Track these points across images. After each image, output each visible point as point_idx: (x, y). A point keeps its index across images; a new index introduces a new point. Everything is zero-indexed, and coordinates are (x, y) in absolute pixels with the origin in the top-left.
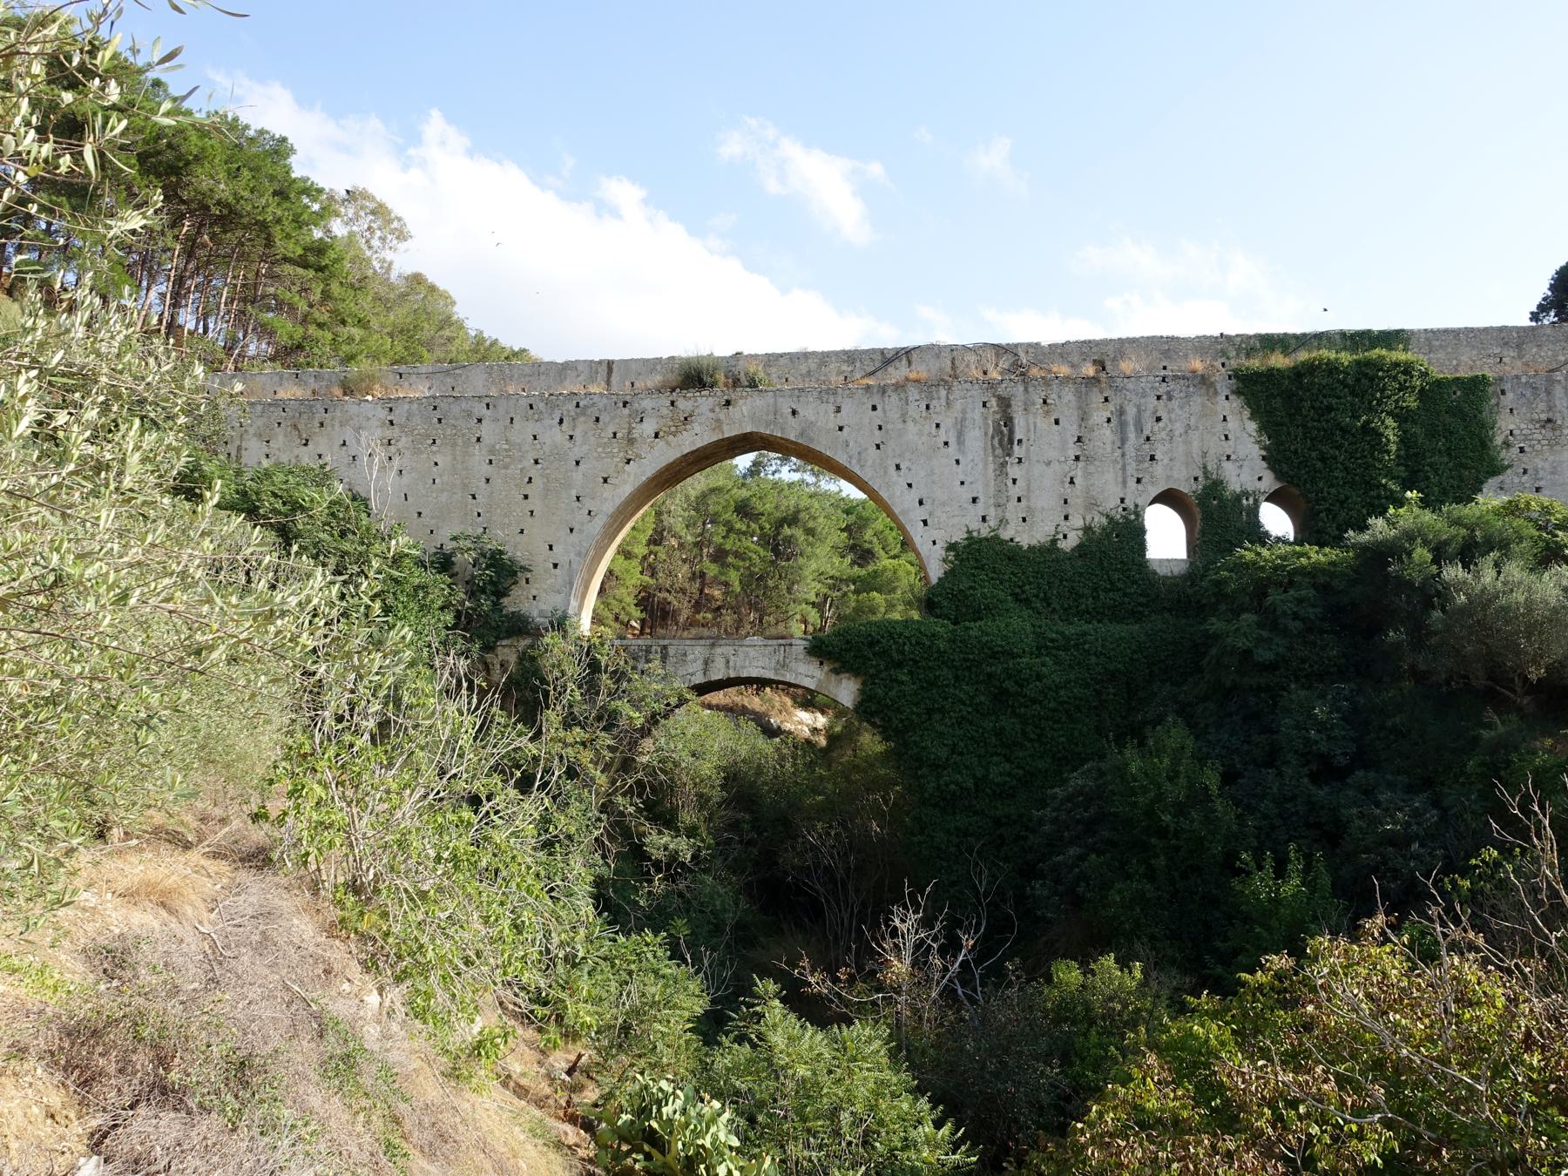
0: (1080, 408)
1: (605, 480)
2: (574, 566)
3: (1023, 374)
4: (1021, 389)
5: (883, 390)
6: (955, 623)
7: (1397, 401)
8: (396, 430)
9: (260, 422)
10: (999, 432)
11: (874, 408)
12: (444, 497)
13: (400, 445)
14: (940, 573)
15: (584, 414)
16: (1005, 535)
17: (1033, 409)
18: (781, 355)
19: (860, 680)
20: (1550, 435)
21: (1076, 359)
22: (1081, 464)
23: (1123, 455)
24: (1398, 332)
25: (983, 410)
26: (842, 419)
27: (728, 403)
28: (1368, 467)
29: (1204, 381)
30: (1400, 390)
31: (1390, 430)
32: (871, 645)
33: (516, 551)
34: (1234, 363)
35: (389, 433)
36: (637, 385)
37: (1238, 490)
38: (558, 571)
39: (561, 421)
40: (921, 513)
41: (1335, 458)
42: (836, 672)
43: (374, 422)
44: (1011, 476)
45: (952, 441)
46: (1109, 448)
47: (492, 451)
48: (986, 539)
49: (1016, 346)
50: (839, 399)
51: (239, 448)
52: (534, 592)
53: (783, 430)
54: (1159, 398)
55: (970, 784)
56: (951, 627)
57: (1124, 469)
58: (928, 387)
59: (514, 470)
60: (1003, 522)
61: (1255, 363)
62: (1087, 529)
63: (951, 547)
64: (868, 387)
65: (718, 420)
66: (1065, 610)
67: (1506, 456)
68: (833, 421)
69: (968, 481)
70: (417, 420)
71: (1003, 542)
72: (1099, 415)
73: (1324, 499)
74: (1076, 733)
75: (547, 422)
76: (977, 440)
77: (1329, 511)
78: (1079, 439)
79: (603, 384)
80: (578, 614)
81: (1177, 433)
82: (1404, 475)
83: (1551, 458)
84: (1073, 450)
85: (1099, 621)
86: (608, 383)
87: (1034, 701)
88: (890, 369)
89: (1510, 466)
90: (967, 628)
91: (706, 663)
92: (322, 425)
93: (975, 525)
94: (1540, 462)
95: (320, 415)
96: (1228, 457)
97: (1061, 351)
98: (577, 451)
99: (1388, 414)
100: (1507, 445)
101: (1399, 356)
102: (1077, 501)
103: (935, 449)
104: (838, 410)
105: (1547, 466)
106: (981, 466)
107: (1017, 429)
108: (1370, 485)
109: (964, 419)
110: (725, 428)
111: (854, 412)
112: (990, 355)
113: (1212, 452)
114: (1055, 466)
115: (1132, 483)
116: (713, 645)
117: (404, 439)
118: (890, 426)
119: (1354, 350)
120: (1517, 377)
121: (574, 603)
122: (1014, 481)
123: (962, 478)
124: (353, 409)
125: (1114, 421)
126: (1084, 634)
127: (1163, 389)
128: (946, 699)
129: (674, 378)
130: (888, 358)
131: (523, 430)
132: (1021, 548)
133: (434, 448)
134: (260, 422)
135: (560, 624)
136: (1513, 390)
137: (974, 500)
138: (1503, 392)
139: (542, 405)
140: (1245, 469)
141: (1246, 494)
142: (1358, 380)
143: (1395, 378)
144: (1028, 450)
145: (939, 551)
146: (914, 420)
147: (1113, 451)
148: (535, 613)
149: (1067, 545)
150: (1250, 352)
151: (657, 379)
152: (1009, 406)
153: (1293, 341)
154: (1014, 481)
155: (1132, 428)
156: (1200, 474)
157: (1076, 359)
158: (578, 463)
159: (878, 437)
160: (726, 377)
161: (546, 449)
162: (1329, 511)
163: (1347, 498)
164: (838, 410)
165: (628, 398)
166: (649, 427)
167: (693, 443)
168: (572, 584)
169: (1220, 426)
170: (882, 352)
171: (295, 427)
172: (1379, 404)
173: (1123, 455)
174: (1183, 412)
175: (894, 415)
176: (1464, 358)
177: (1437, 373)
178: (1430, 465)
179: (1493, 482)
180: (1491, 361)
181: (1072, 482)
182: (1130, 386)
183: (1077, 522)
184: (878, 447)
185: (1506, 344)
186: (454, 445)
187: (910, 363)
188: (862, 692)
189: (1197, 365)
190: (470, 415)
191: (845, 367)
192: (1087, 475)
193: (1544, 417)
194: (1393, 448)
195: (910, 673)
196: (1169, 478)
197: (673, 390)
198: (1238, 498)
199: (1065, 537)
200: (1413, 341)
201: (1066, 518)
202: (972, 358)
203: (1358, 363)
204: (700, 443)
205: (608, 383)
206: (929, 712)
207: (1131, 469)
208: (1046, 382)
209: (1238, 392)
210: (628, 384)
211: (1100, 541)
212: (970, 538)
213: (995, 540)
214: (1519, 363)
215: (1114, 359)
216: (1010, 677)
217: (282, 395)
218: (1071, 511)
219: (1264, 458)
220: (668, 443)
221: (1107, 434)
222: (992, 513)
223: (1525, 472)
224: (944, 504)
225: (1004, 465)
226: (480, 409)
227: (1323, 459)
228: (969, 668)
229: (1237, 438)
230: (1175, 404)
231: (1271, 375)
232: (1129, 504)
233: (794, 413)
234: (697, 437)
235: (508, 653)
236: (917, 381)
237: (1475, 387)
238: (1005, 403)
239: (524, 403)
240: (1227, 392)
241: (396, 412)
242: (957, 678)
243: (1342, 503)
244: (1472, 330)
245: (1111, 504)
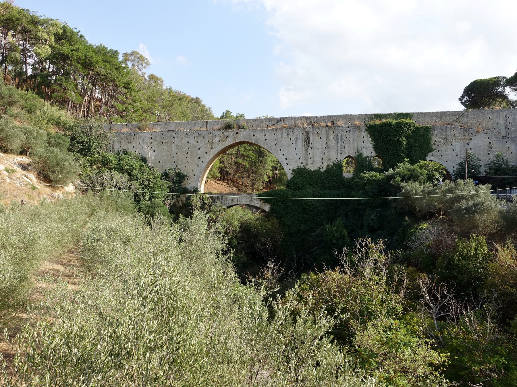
0: (327, 134)
1: (206, 153)
2: (199, 175)
3: (313, 125)
4: (312, 129)
5: (277, 130)
6: (294, 191)
7: (406, 133)
8: (153, 140)
9: (118, 138)
10: (306, 141)
11: (274, 134)
12: (165, 158)
13: (154, 144)
14: (291, 177)
16: (307, 167)
17: (315, 135)
18: (251, 120)
19: (270, 205)
20: (445, 141)
21: (327, 121)
22: (326, 149)
23: (337, 147)
24: (410, 113)
25: (302, 135)
26: (266, 137)
27: (237, 133)
28: (398, 150)
29: (358, 128)
30: (407, 130)
31: (404, 140)
33: (184, 172)
34: (367, 122)
35: (151, 141)
36: (214, 128)
37: (366, 156)
38: (195, 177)
39: (195, 138)
40: (286, 162)
41: (390, 148)
42: (264, 202)
43: (147, 138)
44: (309, 152)
46: (334, 145)
47: (177, 145)
48: (302, 169)
49: (311, 117)
50: (265, 132)
51: (113, 145)
52: (189, 182)
53: (251, 140)
54: (347, 132)
55: (296, 231)
56: (293, 191)
57: (337, 150)
58: (289, 128)
59: (183, 151)
60: (307, 164)
61: (372, 123)
62: (328, 166)
63: (294, 171)
64: (273, 129)
65: (235, 138)
66: (321, 187)
67: (434, 147)
68: (264, 138)
69: (298, 154)
70: (158, 137)
72: (331, 136)
73: (387, 159)
74: (322, 218)
75: (191, 138)
76: (300, 143)
77: (388, 162)
78: (326, 143)
79: (205, 127)
80: (200, 188)
82: (407, 152)
83: (445, 148)
84: (324, 146)
85: (330, 190)
86: (207, 127)
87: (312, 210)
88: (279, 123)
89: (435, 150)
90: (296, 192)
91: (232, 200)
92: (134, 139)
93: (300, 165)
94: (442, 149)
95: (133, 136)
96: (364, 147)
97: (323, 118)
98: (199, 146)
99: (404, 137)
100: (434, 144)
101: (408, 121)
102: (325, 159)
103: (290, 145)
104: (265, 135)
105: (444, 150)
106: (301, 149)
108: (398, 155)
109: (297, 137)
110: (236, 139)
111: (269, 136)
112: (304, 120)
113: (360, 146)
114: (320, 150)
115: (339, 154)
117: (155, 142)
118: (278, 139)
119: (396, 119)
120: (438, 126)
121: (199, 184)
122: (310, 153)
123: (297, 153)
124: (142, 135)
126: (325, 193)
127: (348, 129)
128: (291, 210)
129: (223, 126)
130: (279, 120)
131: (185, 140)
133: (163, 145)
134: (118, 138)
135: (196, 191)
136: (437, 130)
137: (300, 158)
138: (434, 130)
139: (190, 134)
140: (368, 151)
141: (368, 157)
142: (397, 128)
143: (406, 127)
144: (313, 146)
145: (291, 172)
146: (284, 138)
147: (335, 146)
148: (189, 187)
149: (323, 170)
150: (371, 119)
151: (218, 126)
152: (309, 134)
153: (383, 116)
154: (310, 153)
155: (340, 140)
156: (357, 152)
157: (327, 121)
158: (199, 149)
159: (275, 142)
160: (237, 126)
161: (191, 145)
162: (388, 162)
163: (392, 158)
165: (212, 132)
166: (217, 139)
167: (228, 143)
168: (199, 180)
169: (362, 139)
170: (277, 119)
171: (127, 139)
172: (402, 134)
173: (337, 147)
174: (351, 136)
175: (279, 136)
176: (426, 120)
177: (417, 126)
178: (414, 150)
179: (430, 154)
180: (433, 121)
181: (324, 154)
182: (339, 129)
183: (325, 164)
184: (275, 145)
185: (437, 116)
186: (168, 144)
187: (284, 121)
188: (270, 208)
189: (357, 123)
190: (171, 136)
191: (267, 123)
192: (328, 152)
193: (444, 137)
194: (404, 146)
195: (282, 203)
196: (349, 153)
197: (223, 130)
198: (366, 158)
200: (413, 115)
201: (323, 163)
202: (300, 121)
203: (397, 123)
204: (230, 144)
205: (207, 127)
206: (287, 213)
207: (339, 151)
208: (318, 128)
209: (367, 130)
210: (212, 127)
211: (331, 169)
212: (298, 168)
213: (305, 169)
214: (440, 122)
215: (336, 121)
216: (306, 204)
217: (123, 130)
218: (324, 161)
219: (373, 148)
220: (222, 144)
221: (333, 141)
222: (304, 162)
223: (439, 151)
224: (292, 160)
225: (307, 149)
227: (387, 148)
228: (297, 202)
229: (366, 142)
230: (351, 133)
231: (375, 126)
232: (339, 159)
233: (254, 136)
234: (230, 142)
235: (183, 197)
236: (285, 127)
237: (427, 129)
238: (308, 133)
239: (185, 133)
240: (364, 130)
241: (153, 135)
242: (294, 204)
243: (391, 160)
244: (429, 113)
245: (334, 159)
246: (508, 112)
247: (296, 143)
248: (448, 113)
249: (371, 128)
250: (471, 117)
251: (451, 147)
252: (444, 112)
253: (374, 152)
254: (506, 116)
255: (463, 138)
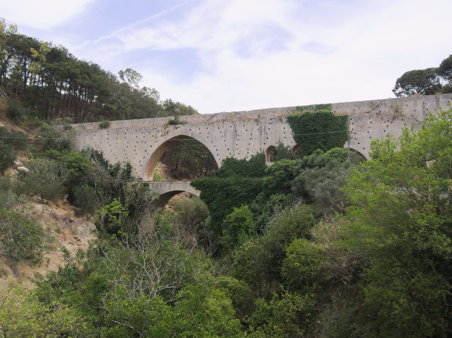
11: (207, 128)
14: (221, 167)
15: (147, 131)
16: (234, 157)
23: (261, 138)
32: (202, 183)
40: (217, 153)
45: (224, 136)
48: (230, 159)
53: (188, 134)
54: (270, 124)
63: (223, 160)
71: (234, 159)
76: (229, 135)
81: (273, 132)
84: (250, 137)
96: (285, 138)
97: (250, 113)
104: (200, 129)
107: (238, 132)
109: (226, 131)
115: (263, 144)
116: (171, 183)
125: (259, 130)
132: (237, 160)
137: (228, 149)
139: (138, 130)
147: (259, 137)
149: (248, 160)
164: (200, 129)
170: (211, 115)
173: (261, 138)
199: (248, 157)
207: (262, 142)
209: (287, 122)
213: (232, 159)
219: (293, 137)
221: (258, 133)
226: (126, 131)
233: (190, 130)
237: (345, 119)
241: (109, 132)
243: (309, 148)
246: (425, 99)
247: (225, 136)
248: (366, 102)
249: (292, 119)
250: (389, 106)
251: (368, 134)
252: (362, 102)
253: (294, 142)
254: (423, 103)
255: (379, 125)
